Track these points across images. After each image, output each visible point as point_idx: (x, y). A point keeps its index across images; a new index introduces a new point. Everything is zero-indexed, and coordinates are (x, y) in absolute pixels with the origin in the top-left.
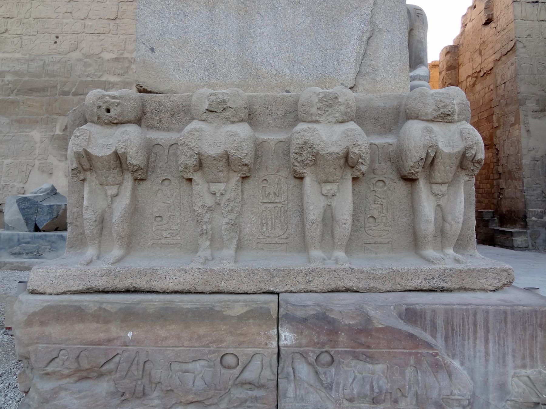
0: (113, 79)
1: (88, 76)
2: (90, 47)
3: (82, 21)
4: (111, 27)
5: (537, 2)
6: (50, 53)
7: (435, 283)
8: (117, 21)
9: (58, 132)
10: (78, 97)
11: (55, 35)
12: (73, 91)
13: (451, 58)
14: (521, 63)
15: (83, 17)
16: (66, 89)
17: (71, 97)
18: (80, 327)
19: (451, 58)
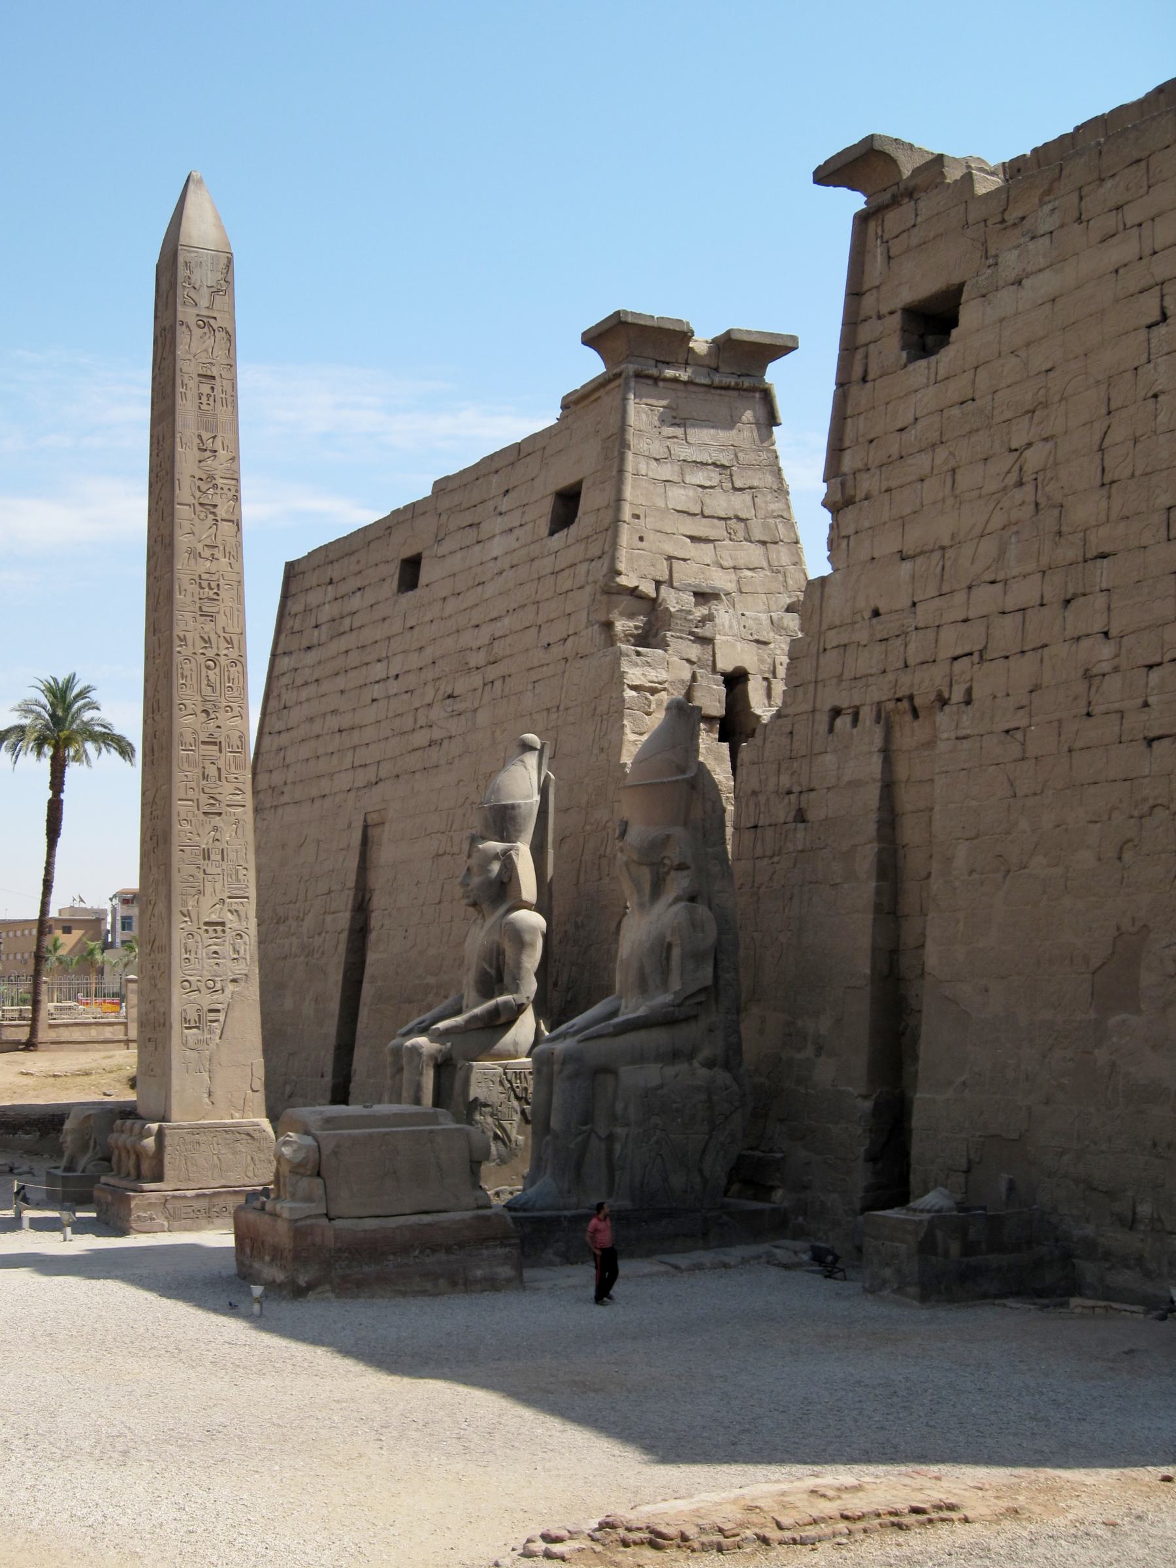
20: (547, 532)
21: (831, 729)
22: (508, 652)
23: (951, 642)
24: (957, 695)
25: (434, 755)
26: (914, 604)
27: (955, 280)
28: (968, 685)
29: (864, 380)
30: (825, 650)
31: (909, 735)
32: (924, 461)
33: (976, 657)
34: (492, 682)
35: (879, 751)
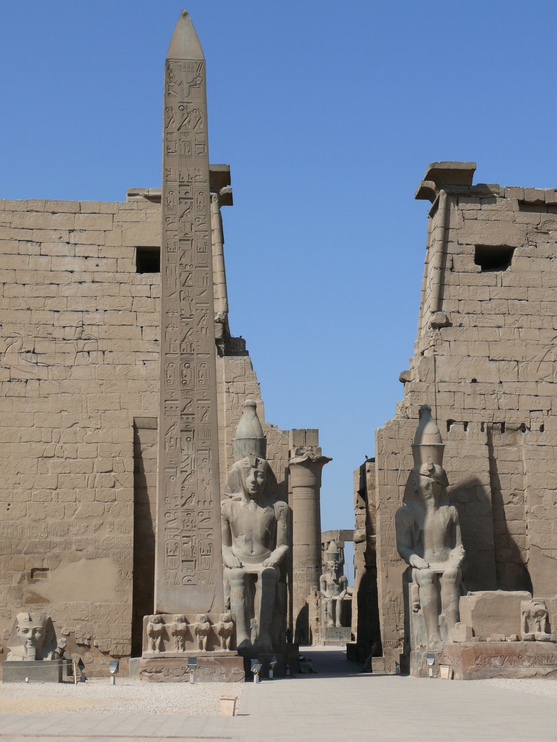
0: (57, 539)
1: (36, 537)
2: (36, 513)
3: (29, 491)
4: (53, 496)
5: (397, 470)
6: (4, 519)
7: (222, 655)
8: (58, 490)
9: (14, 584)
10: (29, 555)
11: (8, 503)
12: (25, 549)
13: (372, 477)
14: (383, 521)
15: (30, 487)
16: (19, 548)
17: (23, 555)
18: (157, 663)
19: (372, 477)
20: (135, 270)
21: (448, 430)
22: (103, 335)
23: (527, 403)
24: (535, 426)
25: (18, 388)
26: (501, 382)
27: (511, 244)
28: (542, 423)
29: (452, 269)
30: (439, 392)
31: (497, 439)
32: (500, 320)
33: (545, 412)
34: (89, 352)
35: (486, 445)
